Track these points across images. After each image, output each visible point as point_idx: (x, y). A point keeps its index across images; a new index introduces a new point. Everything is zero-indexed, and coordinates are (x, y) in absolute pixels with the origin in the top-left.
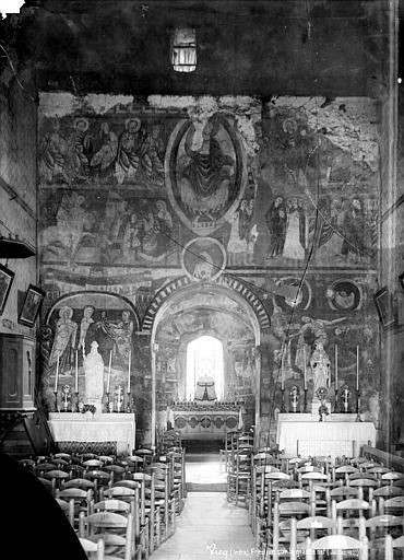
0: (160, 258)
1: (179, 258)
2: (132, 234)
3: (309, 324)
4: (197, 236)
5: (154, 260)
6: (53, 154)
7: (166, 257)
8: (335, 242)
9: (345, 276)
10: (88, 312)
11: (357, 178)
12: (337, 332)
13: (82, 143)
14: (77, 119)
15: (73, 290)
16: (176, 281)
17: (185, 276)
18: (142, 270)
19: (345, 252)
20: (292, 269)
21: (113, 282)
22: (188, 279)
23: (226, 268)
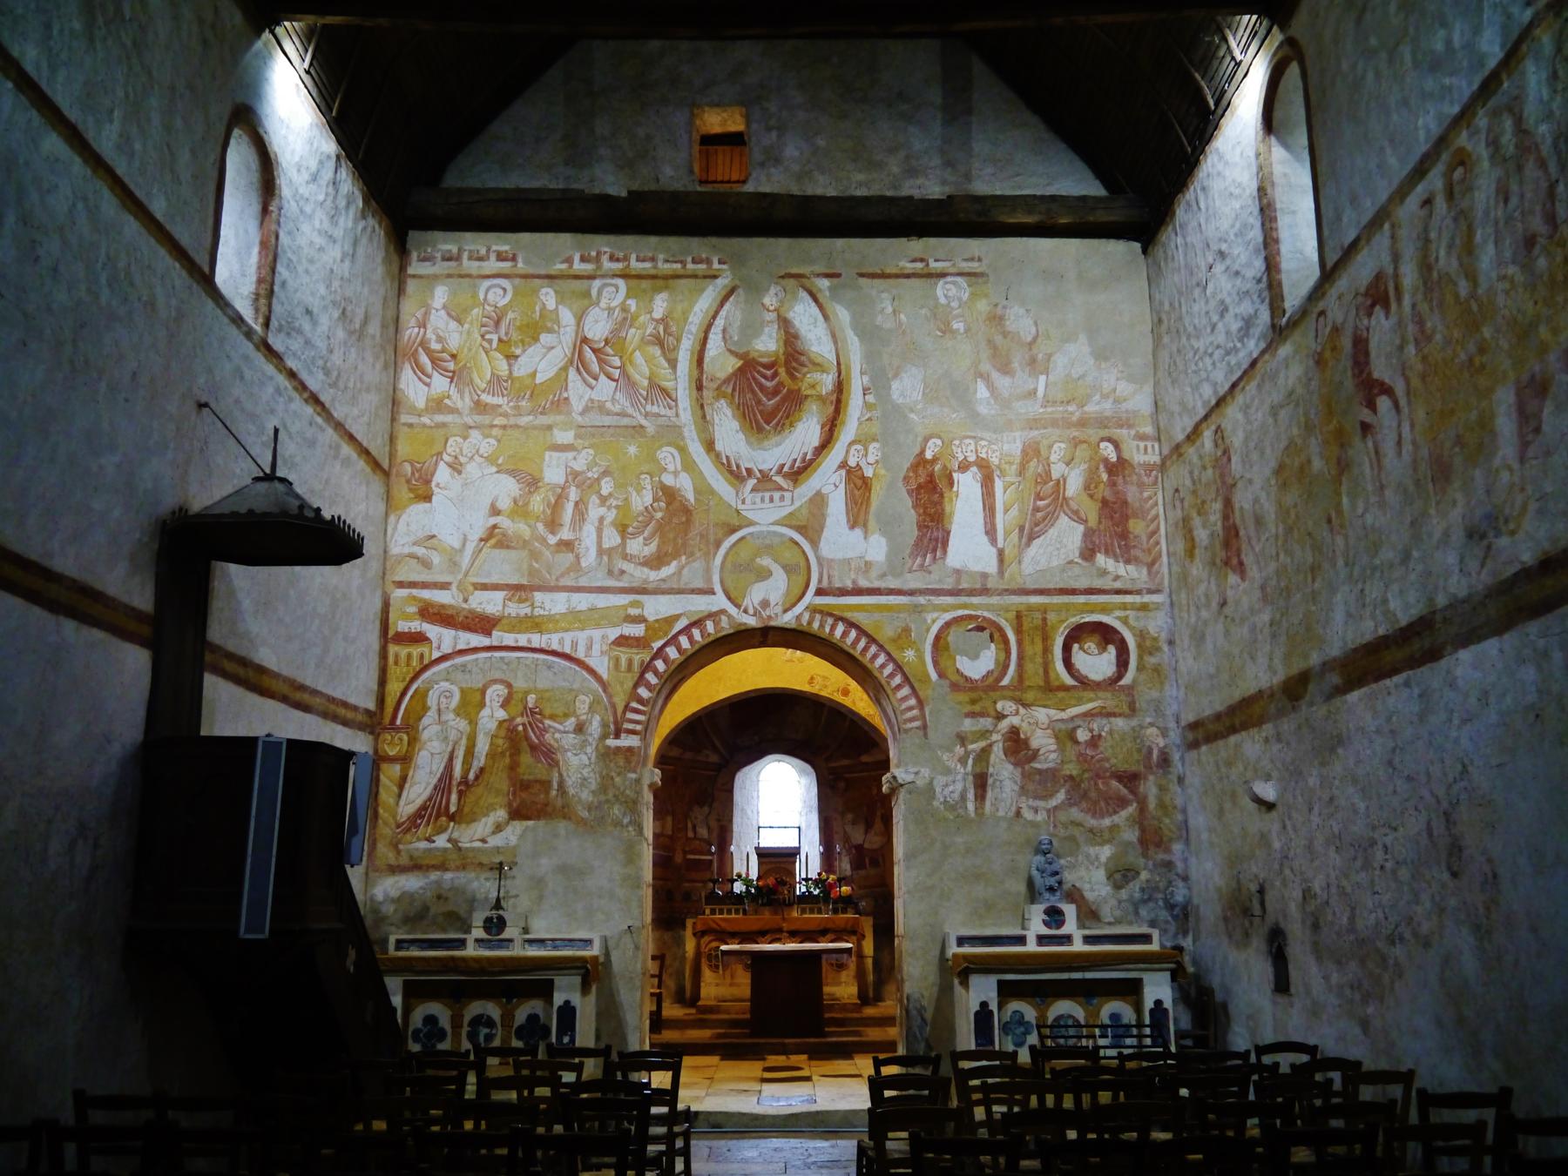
0: (666, 571)
1: (708, 571)
2: (601, 519)
3: (1015, 717)
4: (751, 523)
5: (653, 576)
6: (429, 352)
8: (1066, 536)
9: (1093, 609)
10: (496, 693)
11: (1105, 397)
12: (1082, 735)
14: (487, 283)
16: (698, 623)
17: (723, 612)
18: (623, 600)
19: (1088, 553)
20: (972, 593)
22: (729, 616)
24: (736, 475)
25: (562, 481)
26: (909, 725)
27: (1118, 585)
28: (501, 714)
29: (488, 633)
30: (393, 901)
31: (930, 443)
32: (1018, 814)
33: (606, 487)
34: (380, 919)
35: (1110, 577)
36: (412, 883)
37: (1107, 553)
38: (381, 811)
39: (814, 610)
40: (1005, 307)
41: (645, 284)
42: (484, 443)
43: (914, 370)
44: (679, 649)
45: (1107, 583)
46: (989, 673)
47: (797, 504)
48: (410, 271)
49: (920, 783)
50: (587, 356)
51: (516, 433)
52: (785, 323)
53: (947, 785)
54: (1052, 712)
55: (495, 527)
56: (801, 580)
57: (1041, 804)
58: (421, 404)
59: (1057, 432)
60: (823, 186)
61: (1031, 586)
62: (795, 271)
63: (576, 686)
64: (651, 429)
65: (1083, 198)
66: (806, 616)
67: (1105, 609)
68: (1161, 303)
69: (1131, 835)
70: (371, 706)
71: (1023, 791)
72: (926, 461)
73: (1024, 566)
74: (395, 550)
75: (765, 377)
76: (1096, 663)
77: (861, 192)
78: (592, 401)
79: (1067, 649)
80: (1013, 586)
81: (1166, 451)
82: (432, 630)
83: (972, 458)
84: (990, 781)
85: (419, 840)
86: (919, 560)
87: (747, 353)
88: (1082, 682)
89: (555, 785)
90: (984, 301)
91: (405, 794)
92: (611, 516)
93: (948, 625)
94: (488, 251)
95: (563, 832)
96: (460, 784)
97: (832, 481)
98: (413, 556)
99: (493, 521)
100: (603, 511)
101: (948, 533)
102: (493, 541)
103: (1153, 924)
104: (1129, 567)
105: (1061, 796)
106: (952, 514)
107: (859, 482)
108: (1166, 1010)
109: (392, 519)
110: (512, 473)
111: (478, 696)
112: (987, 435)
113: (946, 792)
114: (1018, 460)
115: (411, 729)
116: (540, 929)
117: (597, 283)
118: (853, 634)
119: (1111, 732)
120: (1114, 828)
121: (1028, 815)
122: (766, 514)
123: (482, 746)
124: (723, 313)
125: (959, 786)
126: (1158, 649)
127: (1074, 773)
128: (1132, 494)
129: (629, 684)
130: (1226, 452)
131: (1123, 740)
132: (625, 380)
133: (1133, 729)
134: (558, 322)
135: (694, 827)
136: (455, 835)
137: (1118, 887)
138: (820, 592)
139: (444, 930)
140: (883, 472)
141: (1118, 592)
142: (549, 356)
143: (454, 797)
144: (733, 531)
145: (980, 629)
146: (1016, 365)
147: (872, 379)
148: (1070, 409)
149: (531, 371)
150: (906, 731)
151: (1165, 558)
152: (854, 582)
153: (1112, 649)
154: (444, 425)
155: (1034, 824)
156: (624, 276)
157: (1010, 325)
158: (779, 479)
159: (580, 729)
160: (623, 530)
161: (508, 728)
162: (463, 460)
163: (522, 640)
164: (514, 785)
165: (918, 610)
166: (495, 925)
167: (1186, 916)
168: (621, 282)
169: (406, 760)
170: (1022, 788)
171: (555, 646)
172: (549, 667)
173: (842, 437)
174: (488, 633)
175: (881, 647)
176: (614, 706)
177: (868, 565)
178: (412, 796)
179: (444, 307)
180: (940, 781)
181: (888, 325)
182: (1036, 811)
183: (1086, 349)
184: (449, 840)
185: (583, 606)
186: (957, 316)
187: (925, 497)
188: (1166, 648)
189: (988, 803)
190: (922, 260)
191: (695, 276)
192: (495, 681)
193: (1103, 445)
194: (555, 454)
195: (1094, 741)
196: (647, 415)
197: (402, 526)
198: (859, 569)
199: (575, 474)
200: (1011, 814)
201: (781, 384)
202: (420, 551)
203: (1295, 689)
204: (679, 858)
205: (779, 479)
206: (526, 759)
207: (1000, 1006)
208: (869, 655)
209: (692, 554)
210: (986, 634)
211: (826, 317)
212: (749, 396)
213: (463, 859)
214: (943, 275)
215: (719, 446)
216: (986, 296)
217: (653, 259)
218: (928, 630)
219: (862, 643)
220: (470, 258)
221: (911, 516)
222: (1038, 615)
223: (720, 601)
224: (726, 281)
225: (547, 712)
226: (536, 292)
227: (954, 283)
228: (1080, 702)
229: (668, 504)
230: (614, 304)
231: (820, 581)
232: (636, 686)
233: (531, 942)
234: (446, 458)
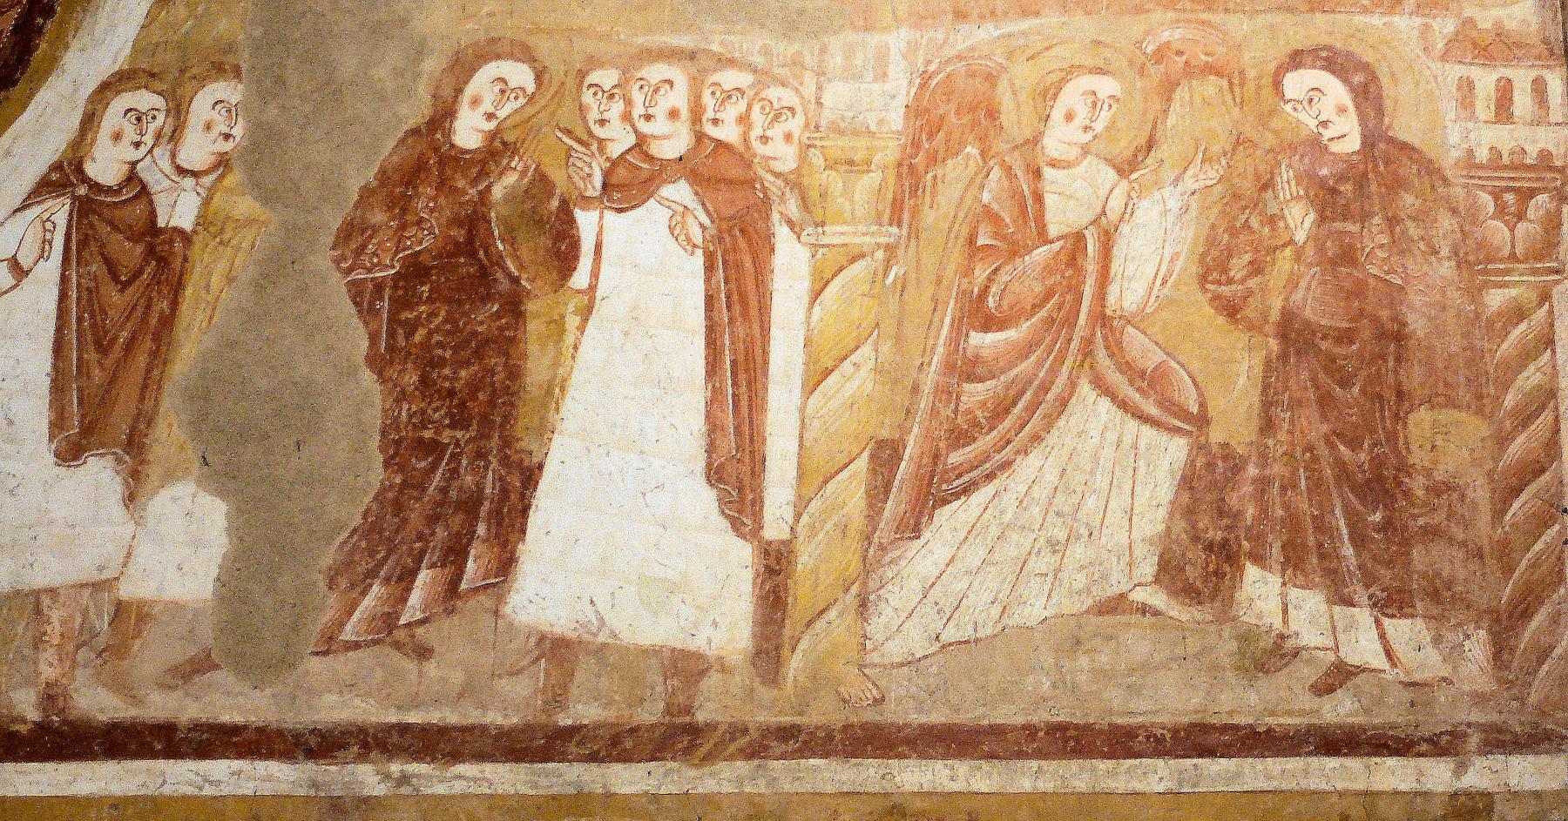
20: (615, 745)
27: (1340, 710)
31: (482, 81)
35: (1309, 673)
37: (1294, 562)
45: (1283, 700)
59: (1083, 26)
61: (905, 711)
72: (454, 159)
80: (822, 714)
83: (672, 143)
86: (374, 598)
101: (531, 476)
104: (1399, 629)
106: (554, 391)
107: (130, 253)
112: (752, 44)
114: (889, 152)
140: (245, 206)
141: (1334, 742)
152: (50, 698)
177: (130, 619)
187: (430, 317)
193: (1297, 83)
198: (84, 637)
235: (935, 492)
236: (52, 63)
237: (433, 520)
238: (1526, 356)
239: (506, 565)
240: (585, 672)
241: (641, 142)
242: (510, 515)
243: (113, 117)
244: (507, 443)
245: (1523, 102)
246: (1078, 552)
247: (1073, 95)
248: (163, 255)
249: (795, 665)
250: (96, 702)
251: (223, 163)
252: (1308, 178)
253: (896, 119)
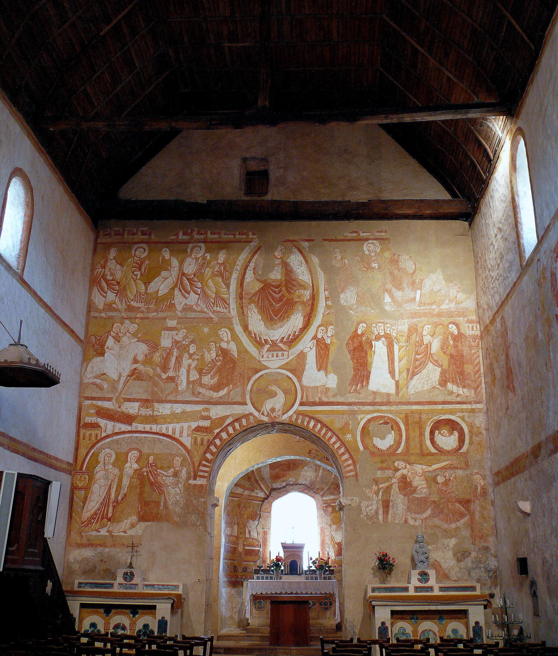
0: (222, 393)
2: (189, 366)
3: (404, 469)
5: (215, 395)
6: (107, 281)
7: (229, 392)
10: (133, 455)
11: (451, 301)
13: (140, 269)
15: (117, 430)
16: (238, 420)
17: (251, 414)
19: (443, 382)
20: (381, 404)
21: (165, 419)
22: (254, 417)
23: (302, 404)
24: (259, 343)
25: (170, 346)
26: (348, 474)
27: (459, 399)
28: (136, 466)
29: (131, 425)
30: (78, 562)
32: (406, 521)
33: (192, 349)
34: (71, 572)
35: (455, 395)
36: (88, 553)
37: (453, 382)
38: (74, 515)
39: (298, 413)
40: (399, 255)
41: (214, 245)
42: (131, 327)
43: (352, 288)
44: (228, 433)
45: (453, 398)
46: (391, 446)
47: (291, 358)
48: (99, 241)
49: (353, 505)
50: (183, 283)
51: (146, 321)
52: (286, 266)
53: (368, 506)
54: (424, 467)
55: (135, 369)
56: (292, 397)
57: (418, 516)
58: (101, 307)
60: (307, 196)
61: (412, 400)
62: (291, 238)
63: (173, 452)
64: (216, 319)
65: (437, 201)
66: (295, 416)
67: (452, 412)
68: (478, 253)
69: (466, 533)
70: (71, 461)
71: (409, 509)
72: (358, 335)
73: (409, 390)
74: (86, 381)
75: (275, 292)
76: (447, 441)
77: (324, 199)
78: (186, 304)
79: (432, 433)
81: (482, 329)
82: (102, 422)
84: (391, 504)
85: (92, 530)
87: (266, 280)
88: (440, 451)
89: (162, 504)
90: (388, 253)
91: (86, 506)
92: (194, 364)
93: (369, 421)
94: (137, 231)
95: (166, 529)
96: (114, 502)
97: (309, 345)
98: (94, 384)
99: (135, 366)
100: (190, 361)
101: (370, 373)
102: (134, 376)
103: (478, 581)
105: (429, 512)
107: (323, 346)
108: (481, 627)
109: (85, 364)
110: (145, 342)
111: (125, 457)
112: (389, 321)
113: (368, 510)
114: (406, 335)
115: (90, 472)
116: (152, 579)
117: (191, 245)
118: (319, 426)
119: (455, 478)
120: (457, 529)
121: (411, 522)
122: (274, 363)
123: (126, 482)
124: (254, 260)
125: (374, 507)
126: (481, 433)
127: (436, 499)
128: (466, 351)
129: (202, 450)
130: (506, 329)
131: (462, 482)
132: (205, 295)
133: (467, 476)
134: (170, 265)
135: (250, 532)
136: (111, 529)
137: (459, 561)
138: (302, 404)
139: (103, 578)
140: (335, 341)
141: (459, 403)
142: (166, 282)
143: (111, 509)
144: (257, 371)
145: (386, 423)
146: (405, 285)
147: (330, 293)
148: (433, 307)
149: (155, 290)
150: (347, 477)
151: (483, 385)
152: (320, 399)
153: (456, 433)
154: (112, 317)
155: (414, 527)
156: (205, 242)
157: (402, 265)
158: (281, 345)
159: (176, 474)
160: (200, 372)
161: (138, 473)
162: (120, 335)
163: (147, 428)
164: (141, 504)
165: (354, 413)
166: (129, 576)
167: (496, 577)
168: (203, 245)
169: (87, 489)
170: (408, 507)
171: (164, 431)
172: (160, 442)
173: (314, 323)
174: (131, 425)
175: (334, 433)
176: (193, 463)
178: (89, 508)
179: (114, 258)
180: (364, 504)
181: (339, 265)
182: (416, 520)
183: (441, 277)
184: (108, 532)
185: (179, 411)
186: (375, 260)
188: (484, 432)
189: (390, 516)
190: (356, 232)
191: (240, 241)
192: (133, 449)
193: (450, 326)
194: (167, 332)
195: (447, 483)
196: (214, 312)
197: (89, 369)
199: (177, 342)
200: (402, 522)
201: (283, 296)
202: (98, 381)
203: (536, 452)
204: (240, 549)
205: (281, 345)
206: (147, 489)
207: (392, 624)
208: (327, 437)
209: (236, 384)
210: (390, 425)
211: (307, 262)
212: (266, 302)
213: (114, 541)
214: (367, 240)
215: (250, 328)
216: (389, 250)
217: (219, 234)
218: (359, 424)
219: (324, 431)
220: (128, 234)
221: (350, 364)
222: (417, 416)
223: (250, 408)
224: (256, 244)
225: (159, 466)
226: (160, 250)
227: (372, 243)
228: (439, 462)
229: (224, 358)
230: (199, 256)
231: (302, 398)
232: (205, 453)
233: (147, 585)
234: (112, 333)
235: (414, 374)
236: (312, 324)
237: (360, 378)
238: (476, 358)
239: (368, 383)
240: (377, 395)
241: (379, 333)
242: (368, 377)
243: (320, 330)
244: (367, 369)
245: (475, 328)
246: (430, 381)
247: (426, 327)
248: (327, 347)
249: (400, 395)
250: (325, 399)
251: (332, 336)
252: (452, 337)
253: (406, 330)
